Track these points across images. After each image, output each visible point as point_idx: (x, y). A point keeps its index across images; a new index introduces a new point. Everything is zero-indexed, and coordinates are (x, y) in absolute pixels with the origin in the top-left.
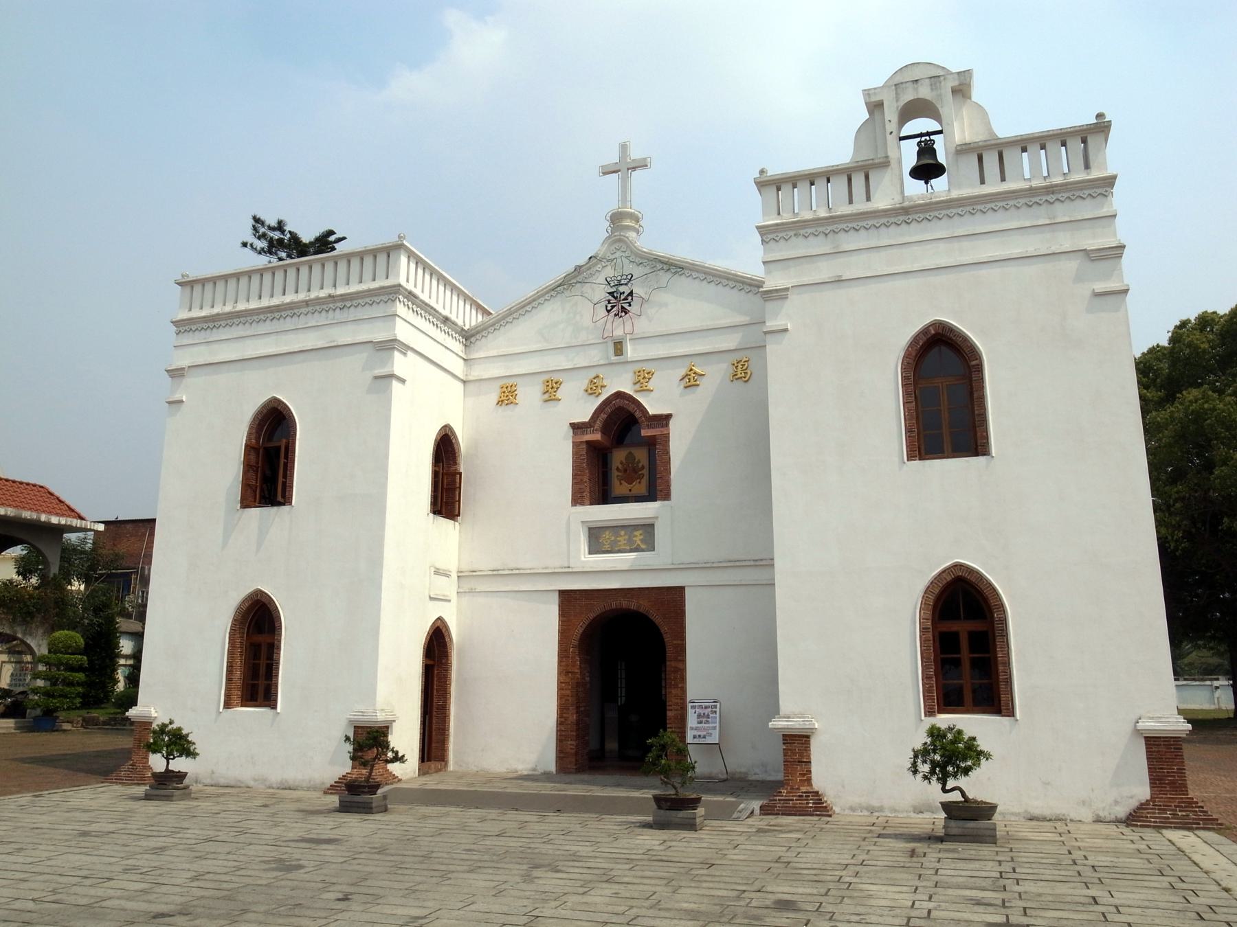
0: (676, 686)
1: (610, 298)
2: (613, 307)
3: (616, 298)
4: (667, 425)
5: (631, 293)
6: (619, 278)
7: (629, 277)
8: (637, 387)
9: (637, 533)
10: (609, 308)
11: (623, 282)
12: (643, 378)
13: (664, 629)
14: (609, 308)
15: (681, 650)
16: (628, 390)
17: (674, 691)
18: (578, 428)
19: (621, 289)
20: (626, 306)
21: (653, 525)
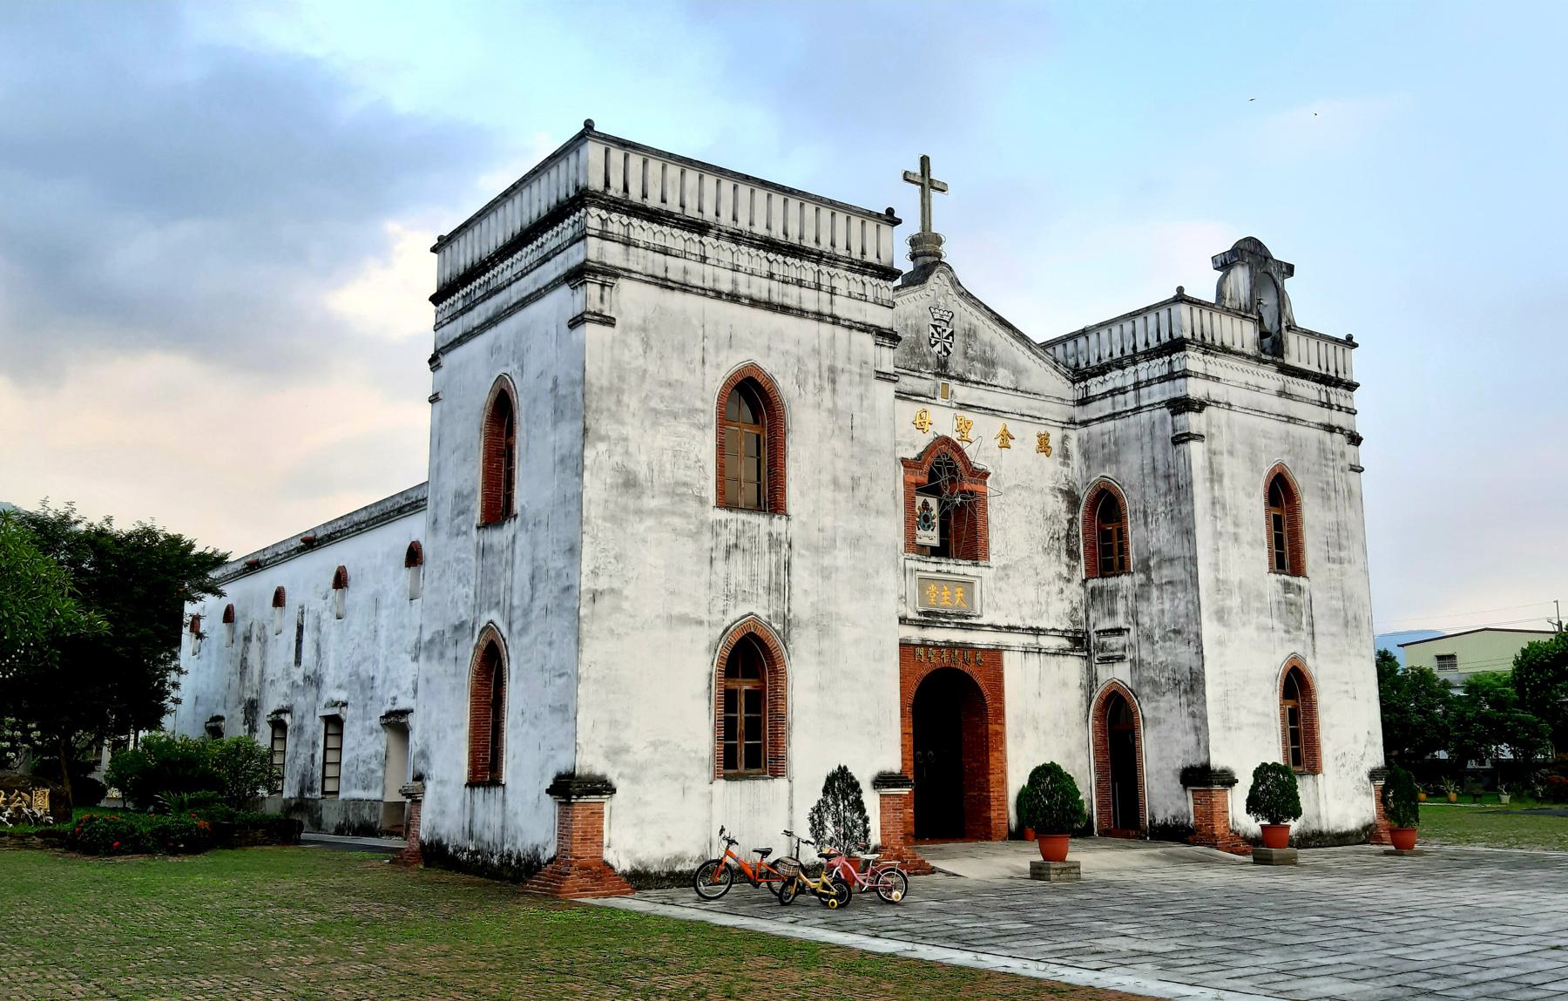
0: (997, 750)
1: (932, 330)
2: (937, 342)
3: (939, 334)
4: (985, 484)
5: (952, 334)
6: (941, 312)
7: (950, 315)
8: (958, 435)
9: (959, 590)
10: (933, 342)
11: (945, 318)
12: (964, 427)
13: (986, 691)
14: (933, 342)
15: (1000, 713)
16: (955, 437)
17: (996, 754)
18: (910, 467)
19: (943, 325)
20: (948, 345)
21: (971, 583)
